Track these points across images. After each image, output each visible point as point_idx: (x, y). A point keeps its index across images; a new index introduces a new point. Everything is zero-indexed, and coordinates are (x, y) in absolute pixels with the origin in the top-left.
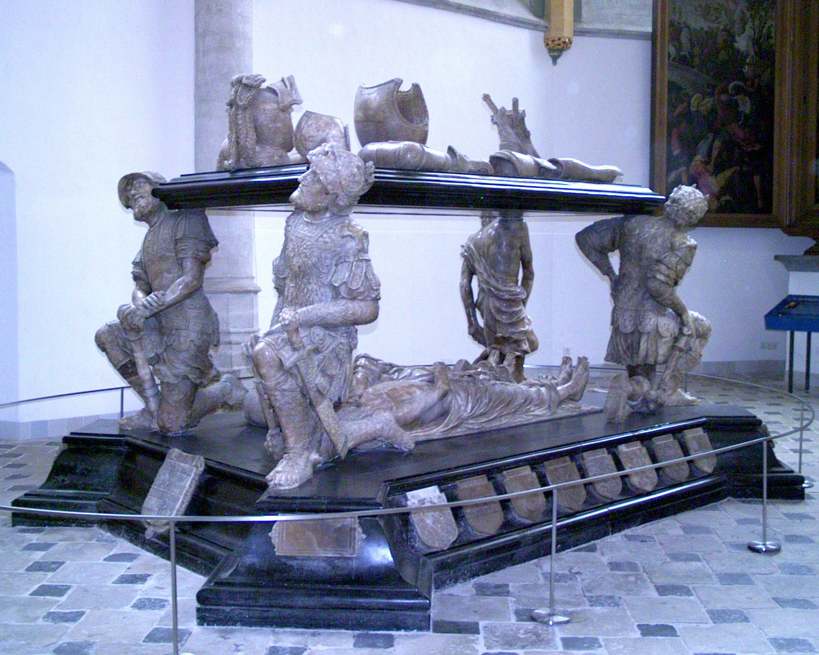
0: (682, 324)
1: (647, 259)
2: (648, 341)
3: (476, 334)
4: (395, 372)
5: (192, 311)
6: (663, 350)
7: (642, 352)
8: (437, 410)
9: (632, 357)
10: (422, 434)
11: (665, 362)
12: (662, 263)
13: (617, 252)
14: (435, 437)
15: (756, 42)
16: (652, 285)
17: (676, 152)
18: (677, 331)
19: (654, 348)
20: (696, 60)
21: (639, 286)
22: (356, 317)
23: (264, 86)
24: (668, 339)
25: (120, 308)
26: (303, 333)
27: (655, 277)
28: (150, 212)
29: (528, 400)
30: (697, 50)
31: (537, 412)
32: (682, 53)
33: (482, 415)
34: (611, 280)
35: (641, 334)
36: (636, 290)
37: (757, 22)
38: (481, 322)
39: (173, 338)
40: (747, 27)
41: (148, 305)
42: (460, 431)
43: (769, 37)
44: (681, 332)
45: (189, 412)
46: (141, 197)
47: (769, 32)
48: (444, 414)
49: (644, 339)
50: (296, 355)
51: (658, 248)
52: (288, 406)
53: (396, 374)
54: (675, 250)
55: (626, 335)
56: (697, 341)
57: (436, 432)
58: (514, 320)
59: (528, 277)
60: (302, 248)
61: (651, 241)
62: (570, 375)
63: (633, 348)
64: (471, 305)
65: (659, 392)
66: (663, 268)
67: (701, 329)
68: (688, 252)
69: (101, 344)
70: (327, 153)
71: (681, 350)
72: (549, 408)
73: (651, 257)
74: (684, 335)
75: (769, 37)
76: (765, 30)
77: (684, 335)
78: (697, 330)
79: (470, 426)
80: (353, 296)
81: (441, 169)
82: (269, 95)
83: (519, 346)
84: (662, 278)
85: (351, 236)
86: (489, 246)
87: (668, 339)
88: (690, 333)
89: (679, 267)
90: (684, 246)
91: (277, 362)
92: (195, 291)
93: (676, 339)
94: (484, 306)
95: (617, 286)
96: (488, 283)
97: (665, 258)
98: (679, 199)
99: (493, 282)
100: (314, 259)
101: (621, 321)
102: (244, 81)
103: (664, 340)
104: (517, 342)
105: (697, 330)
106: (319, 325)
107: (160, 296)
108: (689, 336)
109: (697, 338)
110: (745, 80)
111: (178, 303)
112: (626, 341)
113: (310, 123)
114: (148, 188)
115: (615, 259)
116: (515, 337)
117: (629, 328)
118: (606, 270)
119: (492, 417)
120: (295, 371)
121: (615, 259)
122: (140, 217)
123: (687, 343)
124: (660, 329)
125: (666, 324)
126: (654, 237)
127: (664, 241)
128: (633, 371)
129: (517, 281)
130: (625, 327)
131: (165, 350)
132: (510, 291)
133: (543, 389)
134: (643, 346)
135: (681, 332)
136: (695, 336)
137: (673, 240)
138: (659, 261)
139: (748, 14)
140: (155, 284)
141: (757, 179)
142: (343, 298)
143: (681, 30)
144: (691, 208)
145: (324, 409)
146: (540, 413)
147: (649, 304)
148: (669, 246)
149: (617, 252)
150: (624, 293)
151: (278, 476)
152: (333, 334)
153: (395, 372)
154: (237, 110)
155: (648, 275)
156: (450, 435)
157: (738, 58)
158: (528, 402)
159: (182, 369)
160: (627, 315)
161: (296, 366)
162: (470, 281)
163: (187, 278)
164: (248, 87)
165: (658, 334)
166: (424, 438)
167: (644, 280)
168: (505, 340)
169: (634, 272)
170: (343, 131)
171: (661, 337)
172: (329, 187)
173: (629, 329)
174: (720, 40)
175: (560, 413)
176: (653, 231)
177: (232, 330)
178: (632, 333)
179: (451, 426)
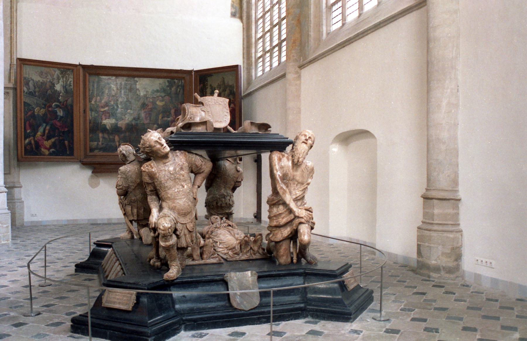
15: (64, 87)
17: (28, 131)
20: (37, 94)
30: (37, 89)
32: (30, 91)
37: (64, 79)
40: (60, 81)
43: (70, 86)
47: (70, 83)
75: (70, 86)
76: (68, 83)
110: (60, 102)
139: (61, 76)
141: (66, 142)
143: (29, 81)
157: (56, 94)
174: (48, 86)
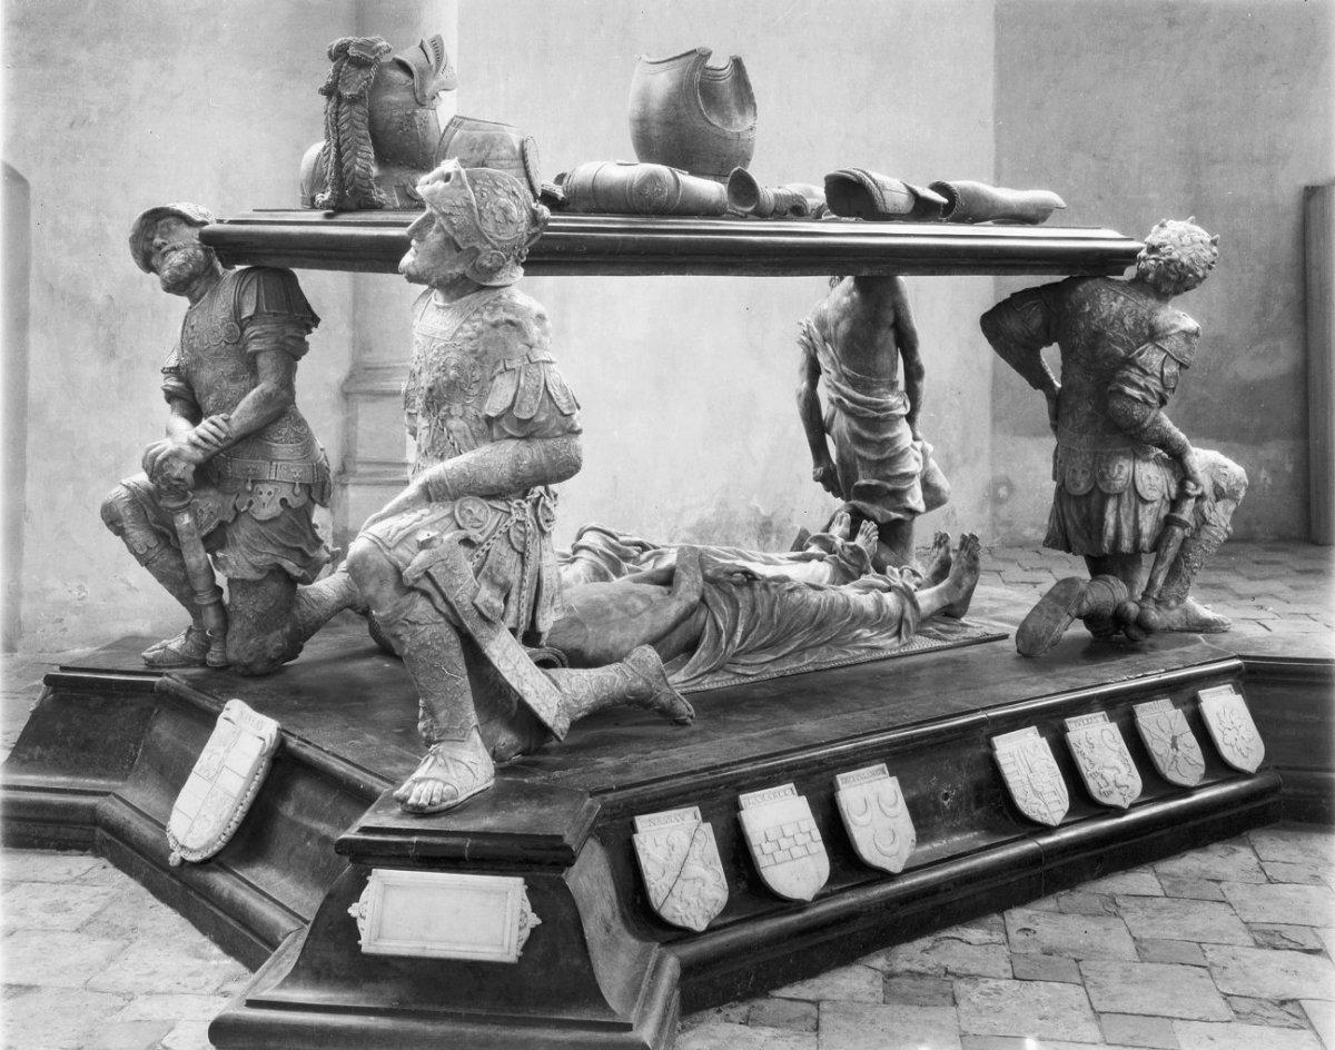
1: (1106, 356)
4: (649, 558)
23: (387, 59)
27: (1122, 392)
29: (861, 619)
53: (652, 562)
54: (1159, 339)
58: (886, 455)
59: (914, 373)
61: (1112, 324)
66: (1134, 375)
68: (1182, 343)
82: (399, 75)
84: (1135, 393)
86: (837, 324)
87: (1156, 505)
89: (1165, 371)
94: (834, 430)
95: (1059, 407)
96: (838, 390)
97: (1140, 354)
102: (352, 52)
104: (898, 495)
106: (470, 493)
107: (220, 422)
116: (889, 486)
126: (1120, 318)
129: (893, 385)
132: (877, 404)
137: (1153, 321)
138: (1129, 362)
140: (209, 402)
148: (1147, 332)
153: (649, 558)
154: (339, 103)
164: (361, 64)
168: (869, 493)
170: (517, 147)
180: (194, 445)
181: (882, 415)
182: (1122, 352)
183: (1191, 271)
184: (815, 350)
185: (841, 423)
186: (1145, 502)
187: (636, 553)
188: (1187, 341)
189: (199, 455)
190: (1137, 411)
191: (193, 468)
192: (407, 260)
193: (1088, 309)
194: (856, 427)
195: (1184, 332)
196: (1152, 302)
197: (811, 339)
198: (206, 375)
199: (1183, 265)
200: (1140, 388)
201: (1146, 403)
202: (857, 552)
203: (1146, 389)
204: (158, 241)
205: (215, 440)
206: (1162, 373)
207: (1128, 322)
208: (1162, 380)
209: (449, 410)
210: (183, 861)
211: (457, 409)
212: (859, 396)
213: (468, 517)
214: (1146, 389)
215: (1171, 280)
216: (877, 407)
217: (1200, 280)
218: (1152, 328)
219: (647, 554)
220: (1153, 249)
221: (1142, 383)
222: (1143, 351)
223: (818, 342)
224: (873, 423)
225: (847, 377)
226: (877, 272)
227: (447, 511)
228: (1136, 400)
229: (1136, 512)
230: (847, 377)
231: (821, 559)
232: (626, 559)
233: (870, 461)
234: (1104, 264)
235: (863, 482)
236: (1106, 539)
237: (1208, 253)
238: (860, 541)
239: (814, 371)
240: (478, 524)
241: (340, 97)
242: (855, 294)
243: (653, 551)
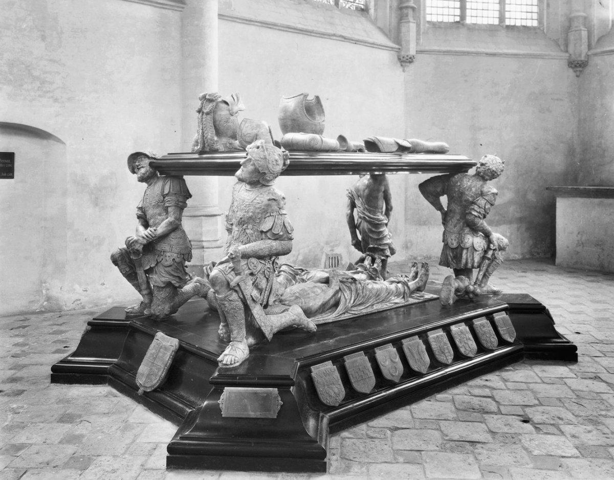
0: (489, 242)
1: (465, 201)
2: (467, 253)
3: (357, 245)
5: (173, 239)
6: (477, 259)
7: (464, 261)
8: (332, 302)
9: (457, 263)
10: (321, 319)
11: (479, 266)
12: (476, 204)
13: (445, 196)
14: (330, 321)
16: (469, 218)
18: (486, 247)
19: (471, 258)
21: (461, 218)
22: (278, 251)
24: (480, 252)
25: (128, 238)
26: (243, 262)
27: (471, 213)
28: (148, 176)
31: (397, 301)
33: (360, 305)
34: (442, 213)
35: (463, 249)
36: (458, 220)
38: (360, 237)
39: (162, 257)
41: (145, 237)
42: (347, 316)
44: (489, 248)
45: (172, 304)
46: (143, 167)
48: (336, 304)
49: (465, 252)
50: (238, 277)
51: (473, 195)
52: (233, 311)
53: (306, 275)
55: (452, 248)
56: (500, 253)
57: (330, 317)
58: (381, 236)
60: (243, 206)
62: (417, 273)
63: (457, 257)
64: (353, 226)
65: (475, 286)
66: (476, 207)
67: (501, 245)
69: (115, 262)
70: (258, 147)
71: (489, 259)
72: (404, 297)
73: (468, 200)
74: (491, 249)
77: (491, 249)
78: (499, 245)
79: (353, 312)
80: (277, 237)
81: (334, 151)
83: (384, 253)
84: (475, 214)
85: (274, 199)
86: (364, 191)
87: (480, 252)
88: (494, 248)
90: (490, 193)
91: (226, 283)
92: (175, 227)
93: (486, 252)
94: (361, 228)
95: (446, 217)
98: (486, 164)
99: (367, 213)
100: (251, 214)
101: (449, 241)
103: (478, 253)
104: (383, 250)
105: (499, 245)
106: (253, 257)
107: (153, 231)
108: (494, 250)
109: (499, 251)
111: (164, 237)
112: (453, 253)
113: (247, 125)
114: (147, 161)
115: (444, 200)
116: (381, 247)
117: (455, 244)
118: (439, 207)
119: (367, 306)
120: (237, 289)
121: (444, 200)
122: (142, 180)
123: (493, 254)
124: (475, 246)
125: (478, 242)
126: (470, 188)
127: (476, 190)
128: (459, 272)
129: (382, 212)
130: (452, 244)
131: (156, 265)
133: (400, 285)
134: (464, 256)
135: (489, 248)
136: (498, 250)
138: (473, 203)
140: (151, 222)
142: (269, 239)
144: (494, 169)
145: (257, 311)
146: (399, 301)
147: (467, 230)
148: (480, 193)
149: (445, 196)
150: (451, 222)
151: (226, 358)
152: (263, 262)
155: (467, 212)
156: (340, 319)
158: (390, 294)
159: (167, 278)
160: (453, 237)
161: (238, 285)
162: (352, 211)
163: (171, 219)
165: (474, 249)
166: (324, 322)
167: (465, 214)
168: (374, 250)
169: (457, 208)
170: (268, 129)
171: (476, 251)
172: (260, 169)
173: (455, 245)
175: (411, 301)
176: (469, 184)
177: (204, 239)
178: (457, 248)
179: (340, 313)
180: (143, 238)
181: (380, 222)
182: (471, 199)
183: (496, 173)
184: (354, 200)
185: (365, 225)
186: (476, 251)
187: (300, 272)
188: (494, 196)
189: (145, 242)
190: (477, 220)
191: (142, 246)
192: (239, 173)
193: (459, 184)
194: (370, 227)
195: (493, 193)
196: (481, 183)
197: (353, 196)
198: (150, 212)
199: (493, 171)
200: (477, 212)
201: (479, 217)
202: (375, 270)
203: (480, 213)
204: (137, 164)
205: (151, 237)
206: (485, 208)
207: (474, 189)
208: (485, 210)
209: (247, 226)
210: (145, 392)
211: (250, 226)
212: (372, 216)
213: (253, 265)
214: (480, 213)
215: (487, 175)
216: (378, 220)
217: (498, 175)
218: (481, 191)
219: (304, 272)
220: (482, 165)
221: (478, 211)
222: (479, 200)
223: (355, 197)
224: (376, 225)
225: (367, 209)
226: (378, 172)
227: (246, 262)
228: (476, 216)
229: (473, 254)
230: (367, 209)
231: (362, 272)
232: (297, 274)
233: (374, 239)
234: (462, 168)
235: (372, 246)
236: (463, 263)
237: (501, 167)
238: (375, 265)
239: (353, 206)
240: (255, 268)
241: (203, 112)
242: (371, 181)
243: (306, 272)
